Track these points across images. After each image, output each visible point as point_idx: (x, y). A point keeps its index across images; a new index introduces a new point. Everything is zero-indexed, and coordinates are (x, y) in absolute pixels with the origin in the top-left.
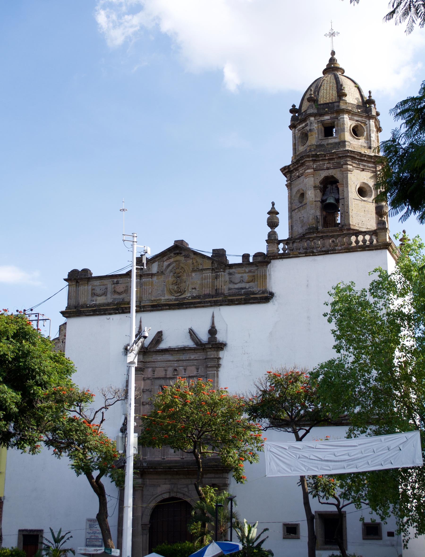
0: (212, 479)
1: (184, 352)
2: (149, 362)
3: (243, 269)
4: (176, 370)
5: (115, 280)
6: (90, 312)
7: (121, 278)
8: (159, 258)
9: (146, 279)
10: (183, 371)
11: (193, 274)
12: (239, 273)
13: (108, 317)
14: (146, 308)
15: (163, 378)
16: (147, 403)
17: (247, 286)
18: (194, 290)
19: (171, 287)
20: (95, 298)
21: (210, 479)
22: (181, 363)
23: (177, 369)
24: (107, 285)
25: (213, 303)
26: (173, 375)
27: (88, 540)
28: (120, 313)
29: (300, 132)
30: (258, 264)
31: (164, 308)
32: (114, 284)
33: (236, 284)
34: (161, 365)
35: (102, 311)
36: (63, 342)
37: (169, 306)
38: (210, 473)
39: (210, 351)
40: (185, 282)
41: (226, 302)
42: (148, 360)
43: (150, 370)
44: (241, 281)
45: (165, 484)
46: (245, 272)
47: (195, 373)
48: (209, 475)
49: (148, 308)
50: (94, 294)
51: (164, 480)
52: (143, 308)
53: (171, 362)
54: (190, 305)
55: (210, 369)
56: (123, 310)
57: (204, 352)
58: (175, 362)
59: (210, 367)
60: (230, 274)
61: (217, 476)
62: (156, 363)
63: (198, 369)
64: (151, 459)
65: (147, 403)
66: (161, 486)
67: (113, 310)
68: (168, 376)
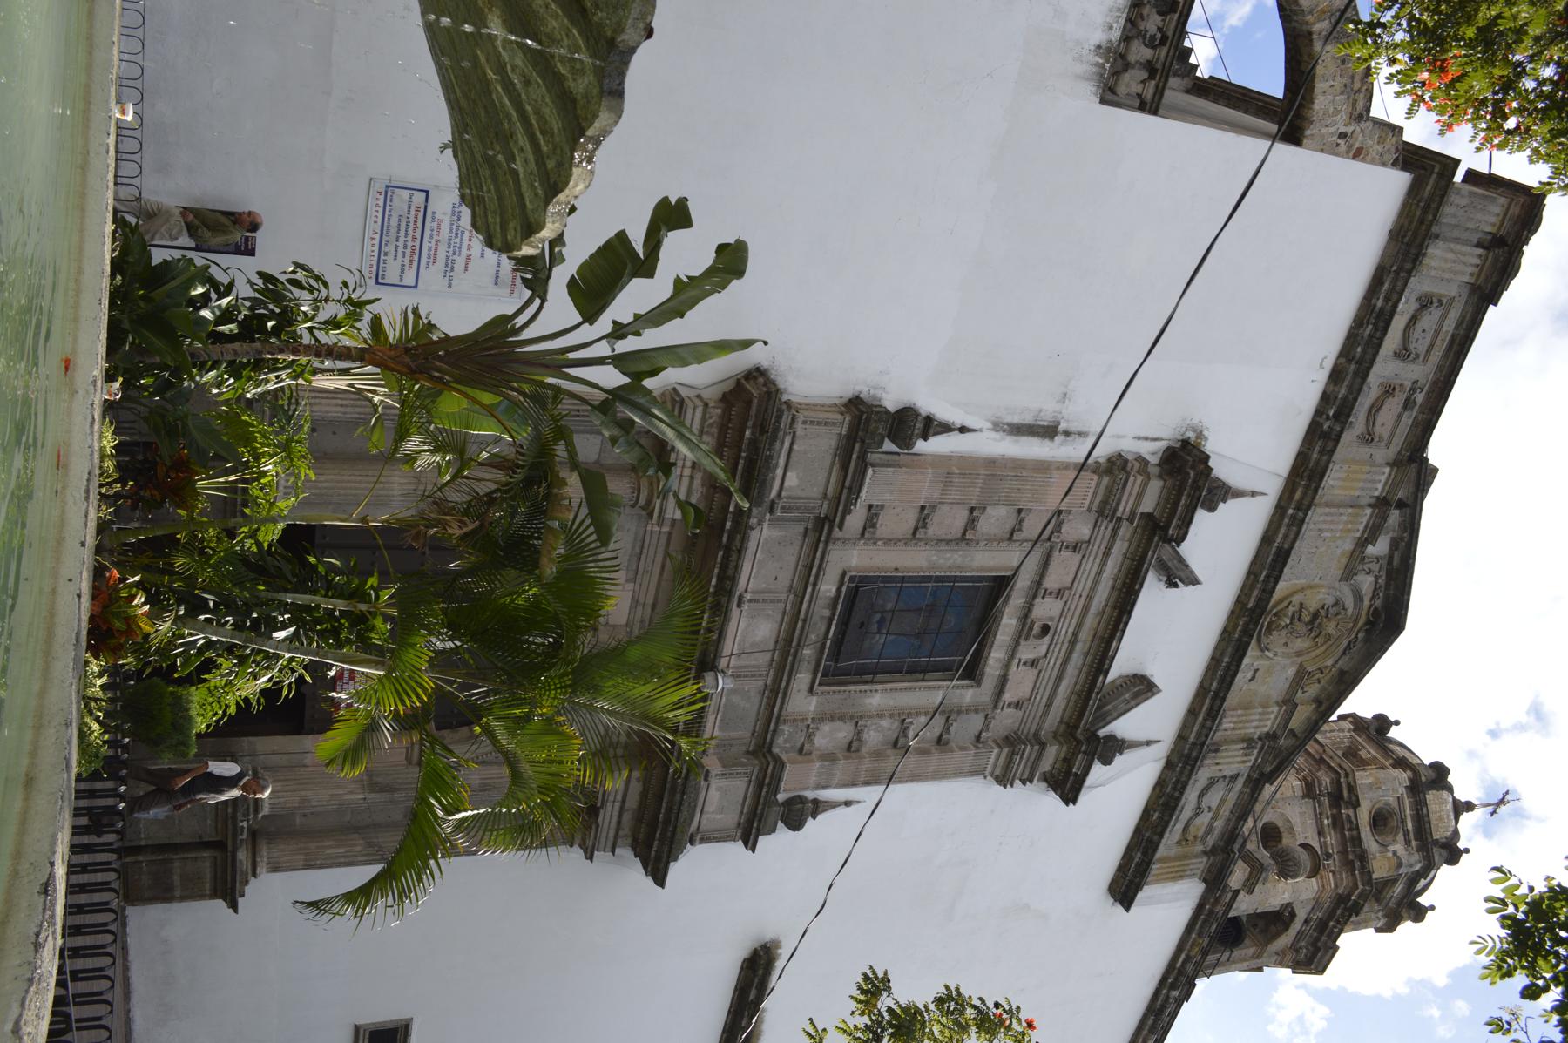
0: (617, 805)
1: (1089, 658)
2: (1115, 533)
3: (1227, 813)
4: (1045, 629)
5: (1420, 398)
6: (1387, 299)
7: (1415, 424)
8: (1396, 561)
9: (1365, 520)
10: (1031, 656)
11: (1291, 671)
12: (1222, 801)
13: (1329, 365)
14: (1289, 525)
15: (1038, 584)
16: (972, 523)
17: (1180, 827)
18: (1249, 675)
19: (1296, 599)
20: (1414, 306)
21: (619, 797)
22: (1060, 650)
23: (1047, 639)
24: (1425, 360)
25: (1191, 750)
26: (1033, 623)
27: (419, 198)
28: (1319, 413)
29: (1394, 804)
30: (1219, 858)
31: (1256, 593)
32: (1413, 390)
33: (1201, 795)
34: (1082, 578)
35: (1364, 351)
36: (1343, 136)
37: (1252, 611)
38: (644, 795)
39: (1058, 755)
40: (1286, 644)
41: (1174, 789)
42: (1125, 531)
43: (1085, 531)
44: (1198, 811)
45: (635, 602)
46: (1214, 819)
47: (1008, 696)
48: (636, 788)
49: (1286, 536)
50: (1425, 303)
51: (650, 601)
52: (1293, 517)
53: (1078, 613)
54: (1222, 679)
55: (1003, 756)
56: (1325, 436)
57: (1061, 722)
58: (1071, 630)
59: (1010, 761)
60: (1234, 778)
61: (627, 817)
62: (1098, 561)
63: (1017, 705)
64: (752, 545)
65: (972, 523)
66: (630, 586)
67: (1345, 399)
68: (1038, 600)
